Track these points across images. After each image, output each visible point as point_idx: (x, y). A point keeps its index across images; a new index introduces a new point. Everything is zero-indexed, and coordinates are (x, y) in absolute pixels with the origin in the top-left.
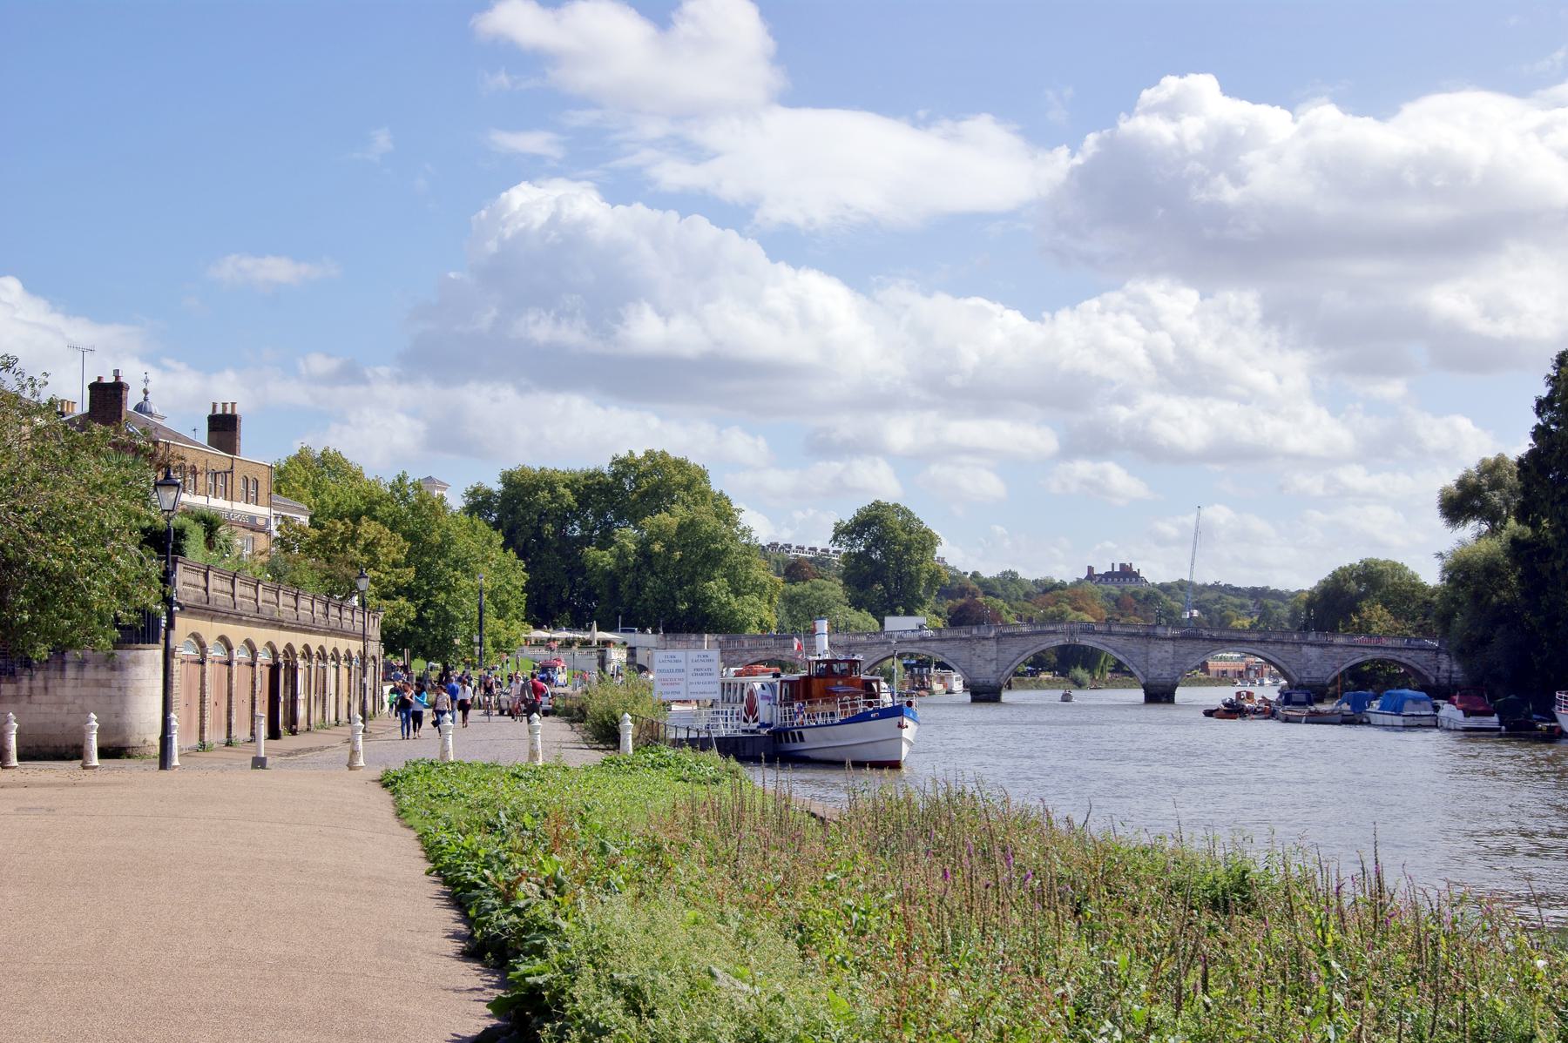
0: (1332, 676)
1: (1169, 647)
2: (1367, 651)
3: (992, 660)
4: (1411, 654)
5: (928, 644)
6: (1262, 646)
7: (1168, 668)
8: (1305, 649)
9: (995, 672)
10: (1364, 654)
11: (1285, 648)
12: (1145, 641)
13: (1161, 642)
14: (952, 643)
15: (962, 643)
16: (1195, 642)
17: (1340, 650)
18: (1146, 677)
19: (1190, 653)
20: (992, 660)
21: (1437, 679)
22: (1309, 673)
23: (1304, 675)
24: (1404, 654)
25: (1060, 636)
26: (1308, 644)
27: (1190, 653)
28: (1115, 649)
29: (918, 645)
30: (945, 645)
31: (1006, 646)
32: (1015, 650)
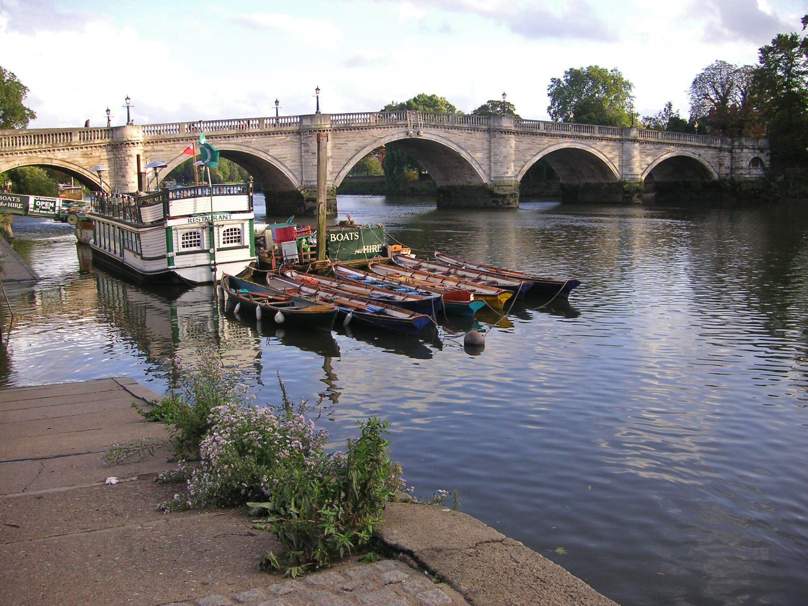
1: (513, 141)
4: (702, 151)
5: (248, 138)
7: (512, 164)
8: (627, 145)
9: (332, 173)
12: (487, 136)
13: (506, 136)
16: (534, 137)
17: (652, 147)
18: (489, 175)
19: (529, 149)
21: (719, 175)
23: (626, 171)
24: (697, 151)
25: (404, 129)
26: (631, 140)
27: (529, 149)
28: (456, 144)
29: (235, 140)
30: (271, 140)
31: (342, 141)
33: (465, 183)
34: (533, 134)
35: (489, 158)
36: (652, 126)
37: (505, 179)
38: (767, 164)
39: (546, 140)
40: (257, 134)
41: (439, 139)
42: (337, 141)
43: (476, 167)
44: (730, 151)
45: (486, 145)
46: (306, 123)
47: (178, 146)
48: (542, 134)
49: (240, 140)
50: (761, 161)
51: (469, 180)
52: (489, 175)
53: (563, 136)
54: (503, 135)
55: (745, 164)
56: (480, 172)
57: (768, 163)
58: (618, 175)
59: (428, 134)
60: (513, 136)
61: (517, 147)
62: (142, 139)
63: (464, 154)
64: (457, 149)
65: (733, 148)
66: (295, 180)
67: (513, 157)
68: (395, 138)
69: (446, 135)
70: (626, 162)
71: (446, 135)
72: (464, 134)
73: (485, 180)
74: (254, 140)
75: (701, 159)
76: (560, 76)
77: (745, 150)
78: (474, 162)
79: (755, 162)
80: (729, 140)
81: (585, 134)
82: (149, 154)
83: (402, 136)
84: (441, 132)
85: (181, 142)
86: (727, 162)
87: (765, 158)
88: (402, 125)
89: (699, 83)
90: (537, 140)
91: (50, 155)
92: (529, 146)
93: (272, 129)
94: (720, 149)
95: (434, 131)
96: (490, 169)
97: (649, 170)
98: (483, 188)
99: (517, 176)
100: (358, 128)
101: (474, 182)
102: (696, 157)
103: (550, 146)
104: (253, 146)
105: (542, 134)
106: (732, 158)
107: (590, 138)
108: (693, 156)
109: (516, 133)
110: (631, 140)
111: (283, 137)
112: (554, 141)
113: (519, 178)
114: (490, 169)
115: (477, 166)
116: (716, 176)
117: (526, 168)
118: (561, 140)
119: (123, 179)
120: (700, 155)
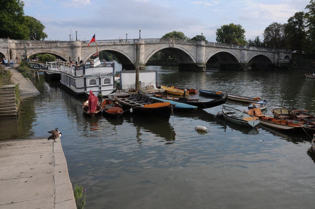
0: (249, 61)
1: (204, 49)
2: (258, 52)
3: (143, 53)
5: (117, 46)
6: (230, 50)
7: (204, 57)
8: (243, 51)
10: (257, 53)
11: (237, 50)
14: (127, 46)
15: (131, 46)
17: (251, 52)
18: (196, 60)
20: (143, 53)
21: (273, 62)
22: (244, 59)
23: (242, 60)
24: (266, 53)
25: (168, 45)
26: (244, 49)
29: (112, 47)
32: (151, 50)
33: (188, 63)
34: (211, 47)
35: (197, 54)
36: (251, 44)
37: (202, 62)
38: (291, 58)
39: (215, 49)
40: (120, 45)
41: (180, 48)
42: (146, 48)
43: (192, 57)
44: (278, 54)
45: (196, 50)
46: (136, 41)
47: (93, 48)
48: (214, 47)
49: (114, 47)
50: (289, 57)
51: (189, 62)
52: (196, 60)
53: (222, 48)
54: (201, 47)
55: (283, 58)
56: (193, 59)
57: (291, 57)
58: (239, 62)
59: (176, 46)
60: (204, 47)
61: (206, 52)
62: (81, 46)
63: (188, 53)
64: (186, 52)
65: (279, 52)
66: (132, 61)
67: (204, 55)
68: (165, 47)
69: (182, 46)
70: (242, 57)
71: (182, 46)
72: (189, 47)
73: (195, 62)
74: (119, 47)
75: (268, 56)
76: (220, 28)
77: (283, 53)
78: (191, 56)
79: (286, 57)
80: (277, 50)
81: (229, 47)
82: (83, 51)
83: (168, 47)
84: (181, 46)
85: (94, 47)
86: (276, 57)
87: (290, 56)
88: (168, 43)
89: (268, 30)
90: (213, 49)
91: (50, 50)
92: (210, 51)
93: (125, 43)
94: (274, 53)
95: (179, 45)
96: (197, 58)
97: (250, 60)
98: (195, 64)
99: (205, 61)
100: (153, 44)
101: (191, 62)
102: (266, 55)
103: (217, 51)
104: (118, 49)
105: (214, 47)
106: (278, 56)
107: (230, 48)
108: (265, 55)
109: (206, 47)
110: (244, 49)
111: (128, 46)
112: (218, 49)
113: (207, 61)
114: (197, 58)
115: (192, 57)
116: (273, 62)
117: (208, 59)
118: (221, 49)
119: (75, 59)
120: (267, 55)
